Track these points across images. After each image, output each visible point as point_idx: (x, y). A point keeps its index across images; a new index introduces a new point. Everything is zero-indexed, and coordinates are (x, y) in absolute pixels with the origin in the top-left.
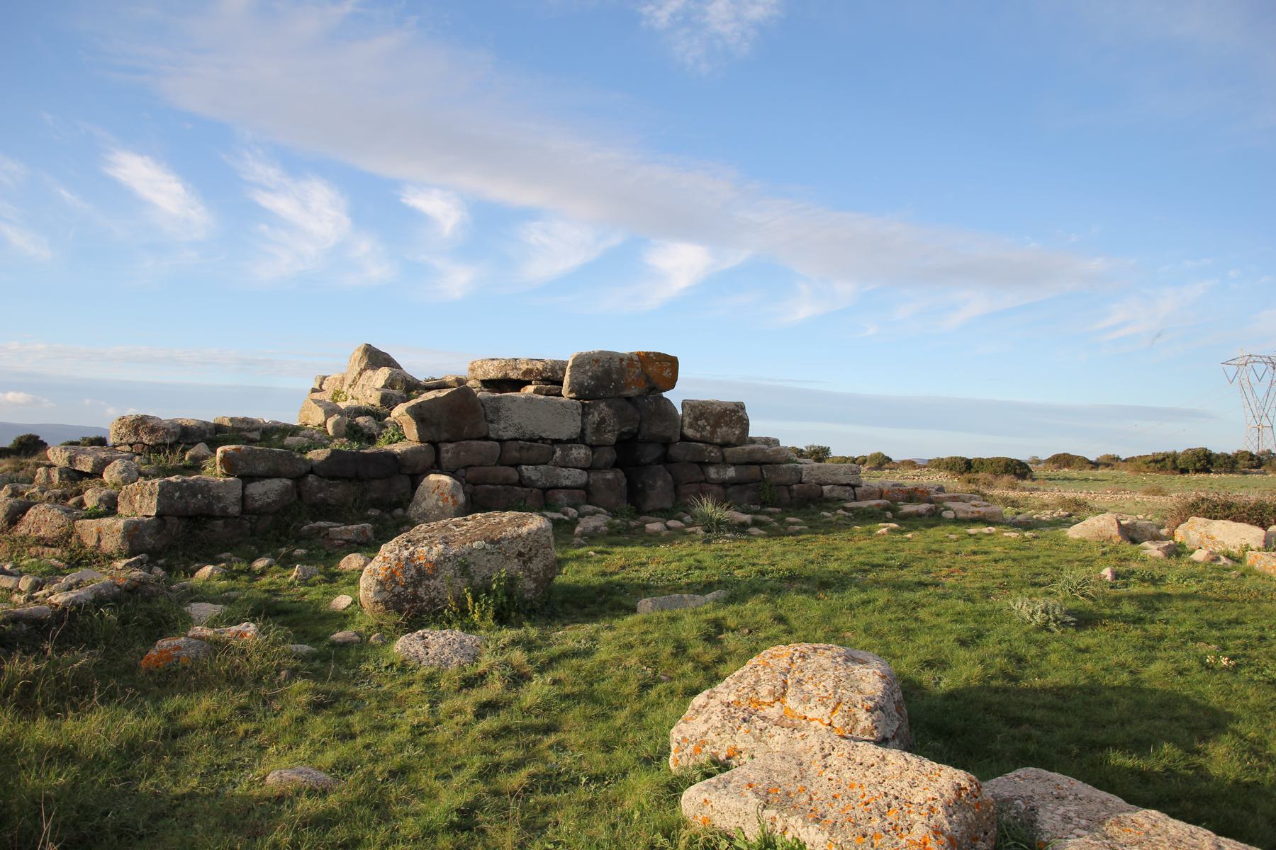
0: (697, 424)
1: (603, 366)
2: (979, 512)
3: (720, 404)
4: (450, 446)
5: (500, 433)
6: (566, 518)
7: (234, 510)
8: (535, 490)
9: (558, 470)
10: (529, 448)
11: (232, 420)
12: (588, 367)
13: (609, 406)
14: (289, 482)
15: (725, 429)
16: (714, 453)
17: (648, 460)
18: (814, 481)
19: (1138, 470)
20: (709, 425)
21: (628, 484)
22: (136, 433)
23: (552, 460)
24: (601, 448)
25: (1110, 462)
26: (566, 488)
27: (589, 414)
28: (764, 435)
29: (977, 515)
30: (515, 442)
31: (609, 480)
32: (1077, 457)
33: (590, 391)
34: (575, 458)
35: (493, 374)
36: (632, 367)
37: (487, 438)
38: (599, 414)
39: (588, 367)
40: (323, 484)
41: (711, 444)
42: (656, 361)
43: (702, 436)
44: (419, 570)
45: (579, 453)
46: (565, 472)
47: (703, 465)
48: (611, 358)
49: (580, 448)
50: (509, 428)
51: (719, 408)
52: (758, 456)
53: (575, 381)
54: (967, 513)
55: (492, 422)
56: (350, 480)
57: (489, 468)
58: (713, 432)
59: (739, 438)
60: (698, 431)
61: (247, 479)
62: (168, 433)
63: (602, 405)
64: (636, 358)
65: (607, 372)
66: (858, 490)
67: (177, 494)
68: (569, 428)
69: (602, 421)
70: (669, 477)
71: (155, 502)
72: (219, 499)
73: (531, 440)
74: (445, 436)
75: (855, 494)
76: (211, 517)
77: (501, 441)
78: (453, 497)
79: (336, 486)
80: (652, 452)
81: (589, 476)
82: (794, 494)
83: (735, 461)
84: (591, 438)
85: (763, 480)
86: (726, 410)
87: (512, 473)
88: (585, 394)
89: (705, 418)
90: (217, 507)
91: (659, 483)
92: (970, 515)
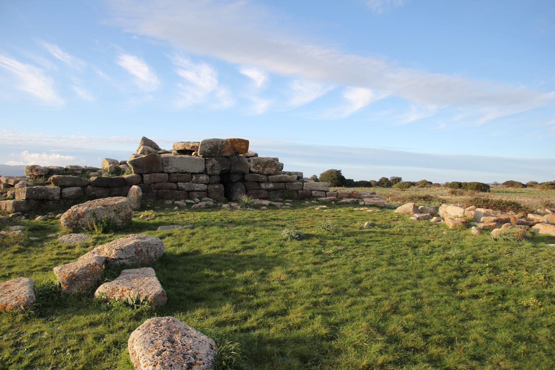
1: (214, 144)
2: (374, 202)
3: (266, 158)
4: (147, 175)
5: (169, 170)
6: (194, 202)
7: (57, 198)
8: (184, 192)
9: (194, 184)
10: (181, 176)
11: (71, 166)
12: (207, 145)
13: (216, 160)
14: (80, 188)
15: (268, 168)
16: (264, 178)
17: (234, 181)
18: (308, 189)
19: (543, 188)
20: (261, 167)
21: (225, 190)
22: (32, 172)
23: (191, 180)
24: (213, 176)
25: (533, 185)
26: (197, 191)
27: (208, 163)
28: (296, 171)
29: (373, 203)
30: (175, 174)
31: (216, 188)
32: (517, 182)
34: (202, 180)
35: (181, 148)
36: (227, 145)
37: (163, 172)
38: (212, 163)
39: (207, 145)
40: (94, 189)
41: (263, 174)
43: (258, 171)
44: (78, 215)
45: (204, 178)
46: (197, 185)
47: (259, 183)
49: (203, 176)
50: (173, 169)
51: (266, 160)
52: (284, 179)
54: (369, 202)
55: (165, 166)
56: (105, 188)
57: (163, 183)
58: (263, 170)
59: (274, 172)
60: (257, 169)
61: (63, 187)
62: (42, 171)
63: (213, 160)
64: (229, 141)
65: (216, 147)
66: (327, 193)
67: (34, 192)
68: (200, 168)
69: (213, 165)
70: (243, 187)
71: (25, 194)
72: (51, 194)
73: (182, 173)
74: (145, 171)
75: (326, 195)
76: (48, 200)
77: (169, 174)
78: (137, 193)
79: (99, 190)
80: (236, 178)
81: (208, 187)
82: (299, 194)
83: (273, 181)
84: (209, 172)
85: (286, 188)
86: (269, 161)
87: (174, 186)
88: (207, 156)
89: (260, 164)
90: (50, 197)
91: (239, 189)
92: (370, 204)
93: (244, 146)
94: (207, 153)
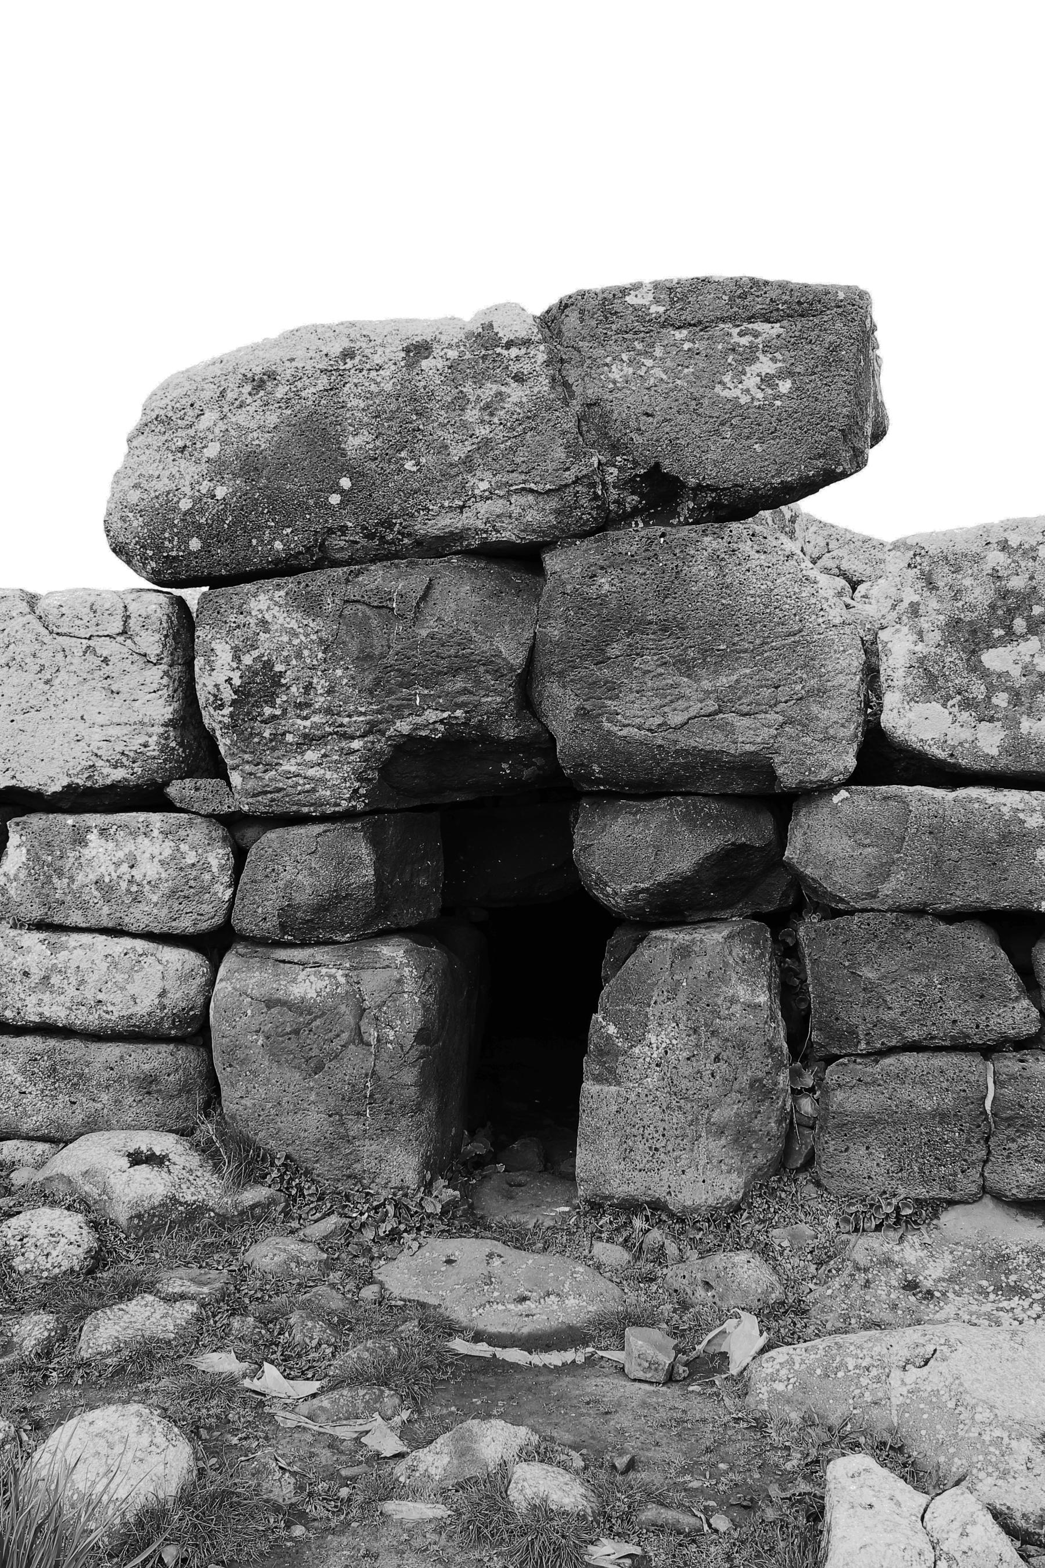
0: (976, 668)
31: (299, 1007)
33: (212, 536)
34: (103, 886)
42: (667, 323)
43: (1016, 745)
48: (348, 354)
53: (134, 497)
60: (984, 713)
93: (765, 365)
94: (190, 525)
